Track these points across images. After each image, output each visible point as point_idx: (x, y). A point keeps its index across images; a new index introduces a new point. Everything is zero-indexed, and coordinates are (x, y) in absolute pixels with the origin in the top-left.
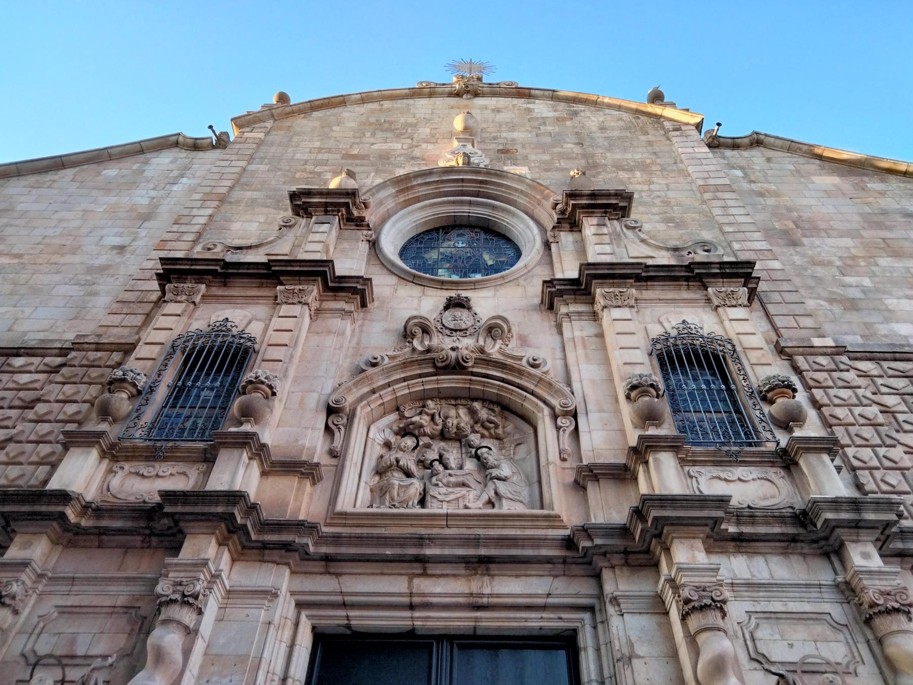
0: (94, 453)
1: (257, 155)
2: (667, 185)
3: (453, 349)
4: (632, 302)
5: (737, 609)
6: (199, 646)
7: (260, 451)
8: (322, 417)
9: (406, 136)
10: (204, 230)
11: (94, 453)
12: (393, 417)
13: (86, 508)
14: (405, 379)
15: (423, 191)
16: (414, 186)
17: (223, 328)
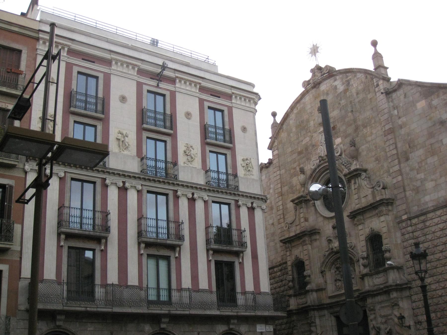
0: (293, 297)
1: (281, 163)
2: (376, 133)
3: (336, 248)
4: (363, 221)
5: (378, 307)
6: (318, 327)
7: (312, 291)
8: (321, 274)
9: (308, 131)
10: (283, 211)
11: (293, 297)
12: (334, 265)
13: (296, 310)
14: (331, 257)
15: (318, 175)
16: (314, 176)
17: (297, 258)
